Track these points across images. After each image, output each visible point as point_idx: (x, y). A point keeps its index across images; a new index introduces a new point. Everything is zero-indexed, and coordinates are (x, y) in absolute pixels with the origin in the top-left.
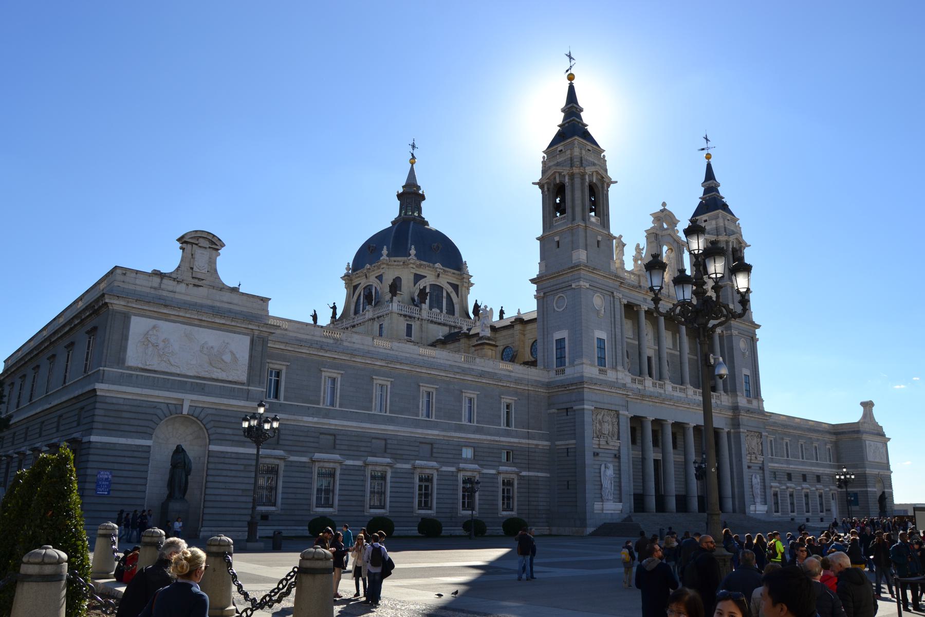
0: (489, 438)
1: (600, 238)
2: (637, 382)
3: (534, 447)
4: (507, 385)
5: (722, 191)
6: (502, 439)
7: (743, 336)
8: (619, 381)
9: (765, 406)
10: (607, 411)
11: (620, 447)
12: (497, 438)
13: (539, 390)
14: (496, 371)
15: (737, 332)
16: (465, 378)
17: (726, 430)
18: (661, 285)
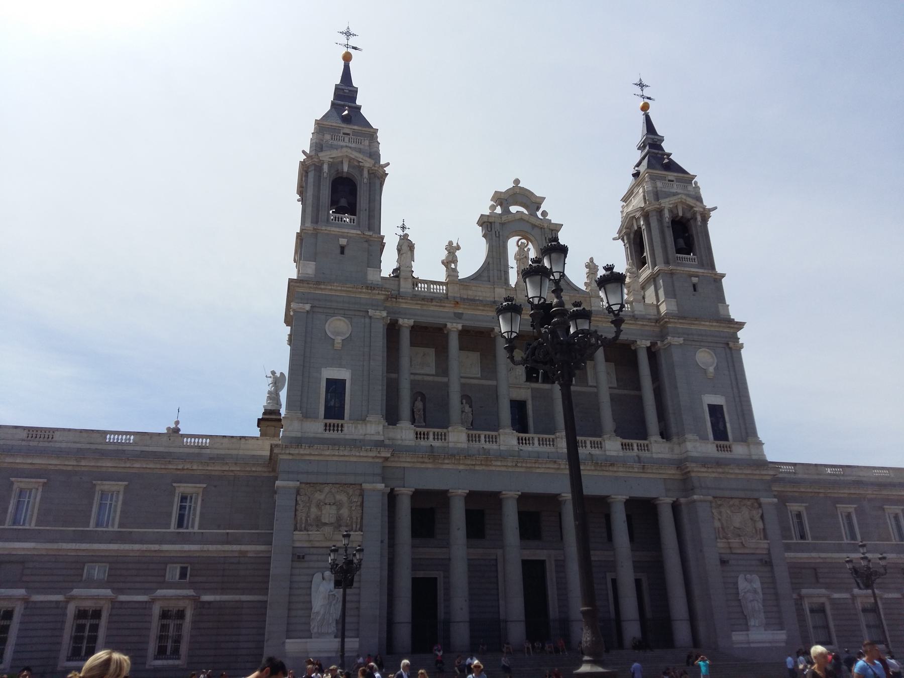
0: (137, 547)
1: (343, 241)
2: (431, 437)
3: (236, 555)
4: (185, 468)
5: (666, 146)
6: (165, 547)
7: (702, 344)
8: (368, 438)
9: (766, 452)
10: (338, 486)
11: (362, 542)
12: (156, 547)
13: (254, 469)
14: (172, 450)
15: (682, 339)
16: (99, 464)
17: (669, 500)
18: (621, 303)
